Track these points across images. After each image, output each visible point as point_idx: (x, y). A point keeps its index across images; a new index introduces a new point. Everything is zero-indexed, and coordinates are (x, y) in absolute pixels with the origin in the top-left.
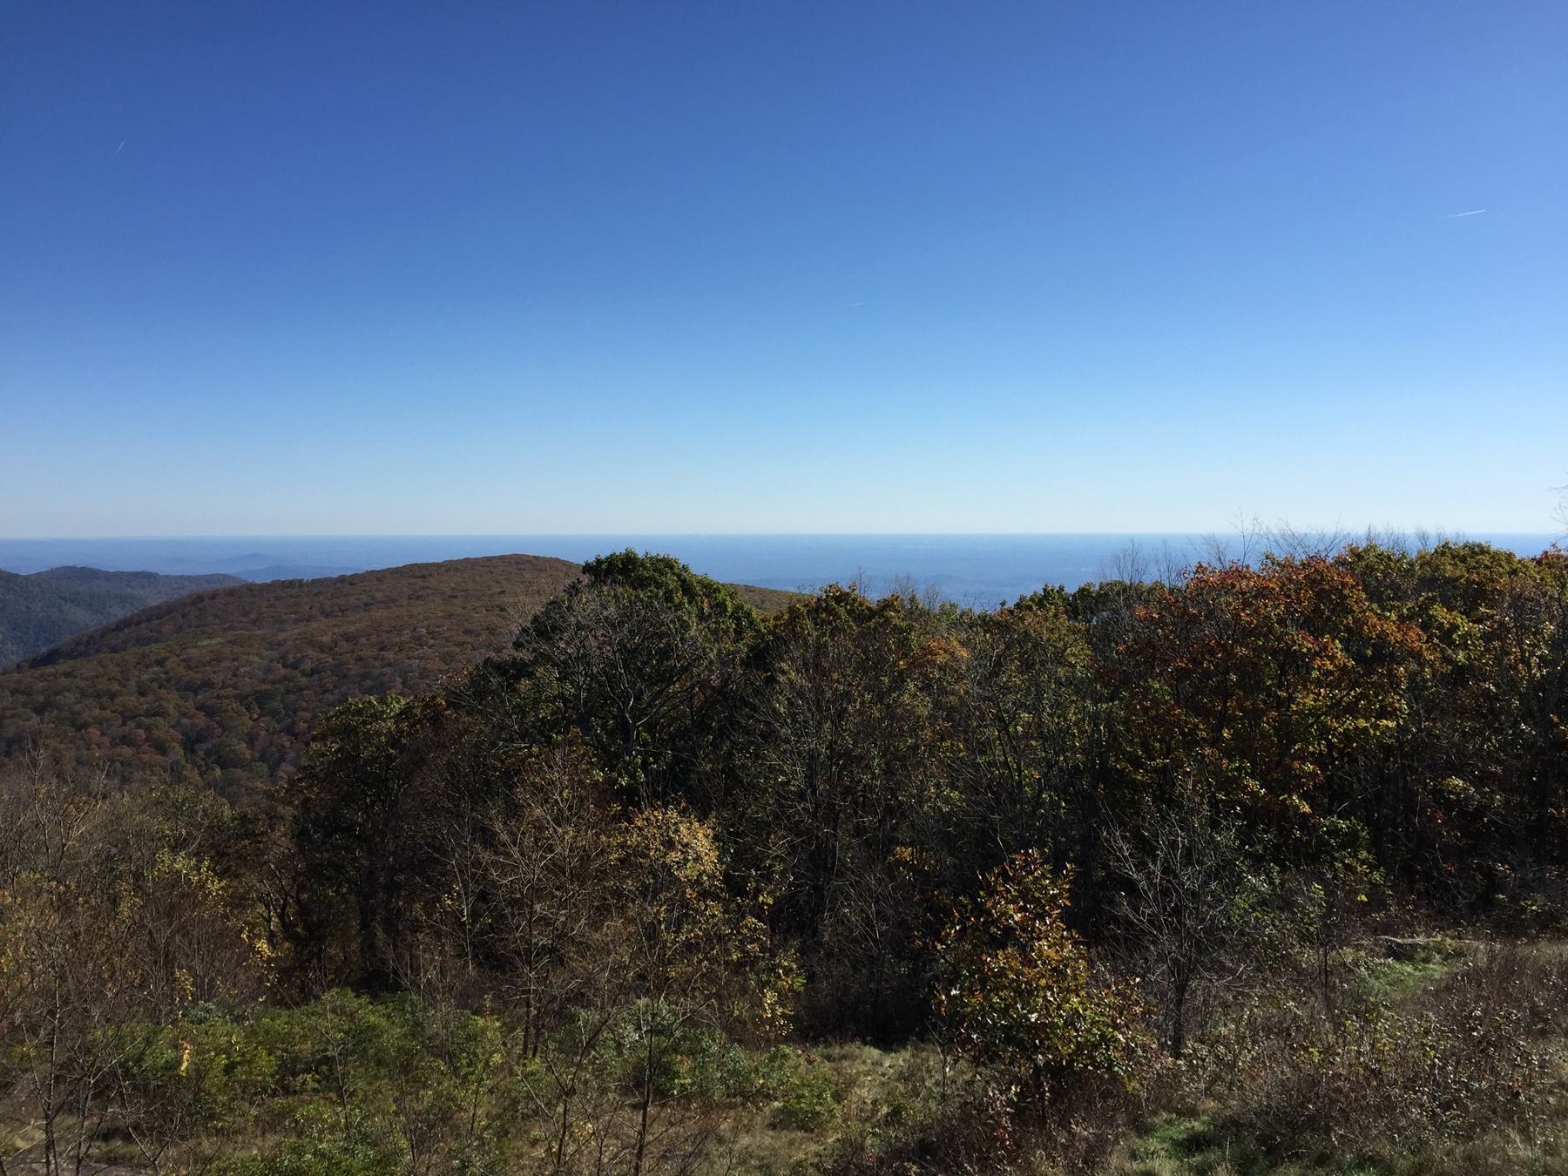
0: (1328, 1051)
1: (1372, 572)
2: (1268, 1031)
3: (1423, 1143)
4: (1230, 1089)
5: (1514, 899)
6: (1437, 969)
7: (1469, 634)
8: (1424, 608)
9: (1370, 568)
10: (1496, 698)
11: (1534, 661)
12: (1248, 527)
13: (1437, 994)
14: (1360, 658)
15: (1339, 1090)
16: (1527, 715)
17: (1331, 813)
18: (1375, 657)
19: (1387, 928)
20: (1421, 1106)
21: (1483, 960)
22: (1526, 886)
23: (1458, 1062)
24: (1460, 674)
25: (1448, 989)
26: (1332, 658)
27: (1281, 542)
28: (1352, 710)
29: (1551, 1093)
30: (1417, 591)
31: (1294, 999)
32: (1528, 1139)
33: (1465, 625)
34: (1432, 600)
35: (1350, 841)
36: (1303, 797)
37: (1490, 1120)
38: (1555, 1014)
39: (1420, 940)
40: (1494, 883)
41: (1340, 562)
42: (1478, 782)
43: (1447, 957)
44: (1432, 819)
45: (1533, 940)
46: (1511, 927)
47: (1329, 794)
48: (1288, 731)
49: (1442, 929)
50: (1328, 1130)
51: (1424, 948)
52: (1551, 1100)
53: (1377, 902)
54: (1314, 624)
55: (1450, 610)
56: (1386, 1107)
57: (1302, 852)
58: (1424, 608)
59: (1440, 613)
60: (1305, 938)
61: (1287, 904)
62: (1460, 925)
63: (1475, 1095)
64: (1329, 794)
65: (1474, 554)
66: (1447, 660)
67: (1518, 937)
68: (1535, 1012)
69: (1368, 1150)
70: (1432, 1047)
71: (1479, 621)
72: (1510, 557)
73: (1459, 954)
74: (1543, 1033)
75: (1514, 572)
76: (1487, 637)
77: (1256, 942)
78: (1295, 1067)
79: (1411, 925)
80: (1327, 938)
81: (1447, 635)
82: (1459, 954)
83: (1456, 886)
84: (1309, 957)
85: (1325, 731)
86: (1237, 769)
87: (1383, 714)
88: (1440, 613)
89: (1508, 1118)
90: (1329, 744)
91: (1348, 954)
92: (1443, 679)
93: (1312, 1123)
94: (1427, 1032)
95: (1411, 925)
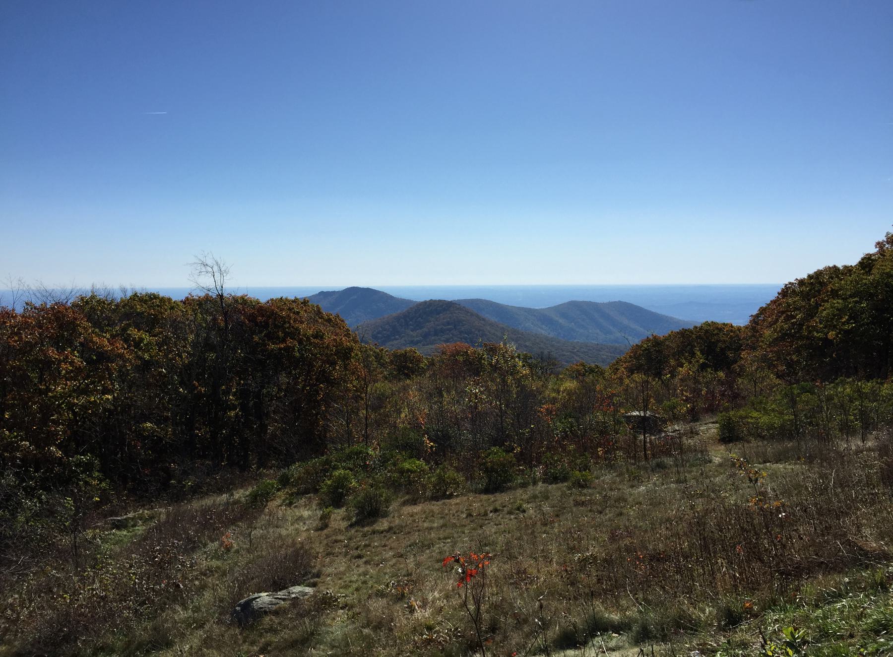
0: (75, 593)
1: (95, 310)
2: (38, 592)
3: (129, 628)
4: (16, 635)
5: (179, 482)
6: (140, 529)
7: (149, 343)
8: (124, 330)
9: (93, 309)
10: (165, 376)
11: (184, 355)
12: (15, 285)
13: (139, 544)
14: (89, 362)
15: (82, 614)
16: (182, 383)
17: (78, 453)
18: (98, 361)
19: (113, 513)
20: (129, 608)
21: (163, 517)
22: (185, 473)
23: (148, 578)
24: (145, 366)
25: (145, 539)
26: (72, 363)
27: (38, 295)
28: (85, 391)
29: (197, 579)
30: (121, 321)
31: (55, 569)
32: (185, 608)
33: (147, 338)
34: (129, 325)
35: (88, 467)
36: (59, 447)
37: (165, 604)
38: (199, 537)
39: (130, 515)
40: (169, 475)
41: (75, 305)
42: (158, 423)
43: (146, 521)
44: (135, 446)
45: (190, 501)
46: (178, 497)
47: (76, 440)
48: (47, 410)
49: (143, 506)
50: (76, 639)
51: (132, 519)
52: (197, 583)
53: (105, 499)
54: (59, 342)
55: (139, 330)
56: (111, 614)
57: (63, 480)
58: (124, 330)
59: (134, 333)
60: (64, 531)
61: (52, 513)
62: (152, 501)
63: (157, 593)
64: (76, 440)
65: (152, 300)
66: (139, 357)
67: (182, 501)
68: (189, 539)
69: (100, 644)
70: (134, 574)
71: (155, 336)
72: (170, 300)
73: (151, 518)
74: (193, 549)
75: (172, 308)
76: (160, 345)
77: (32, 540)
78: (54, 608)
79: (125, 508)
80: (76, 526)
81: (138, 344)
82: (151, 518)
83: (149, 481)
84: (66, 541)
85: (71, 407)
86: (16, 437)
87: (106, 391)
88: (134, 333)
89: (175, 600)
90: (74, 414)
91: (89, 534)
92: (137, 368)
93: (66, 639)
94: (131, 566)
95: (125, 508)
